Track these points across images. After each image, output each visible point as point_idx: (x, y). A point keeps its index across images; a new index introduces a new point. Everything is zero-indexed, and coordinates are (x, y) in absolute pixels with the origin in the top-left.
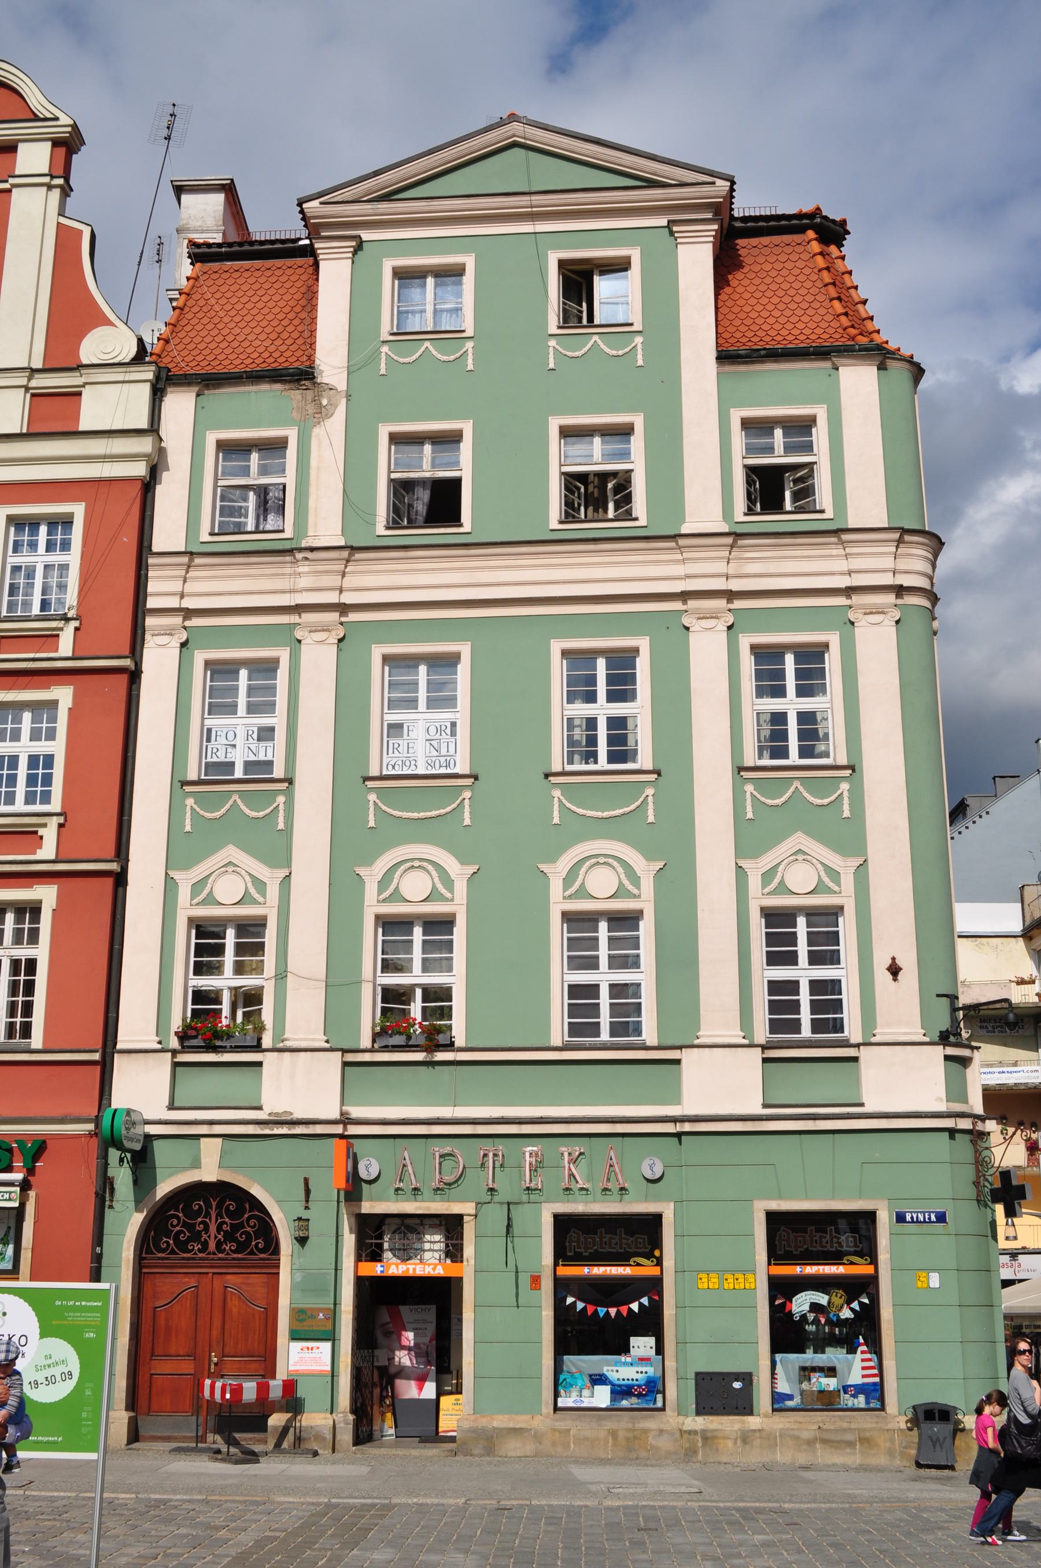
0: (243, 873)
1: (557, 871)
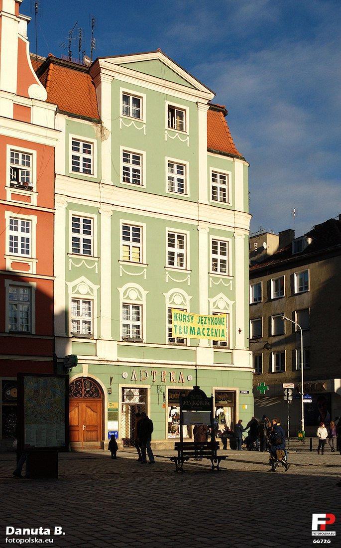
1: (167, 295)
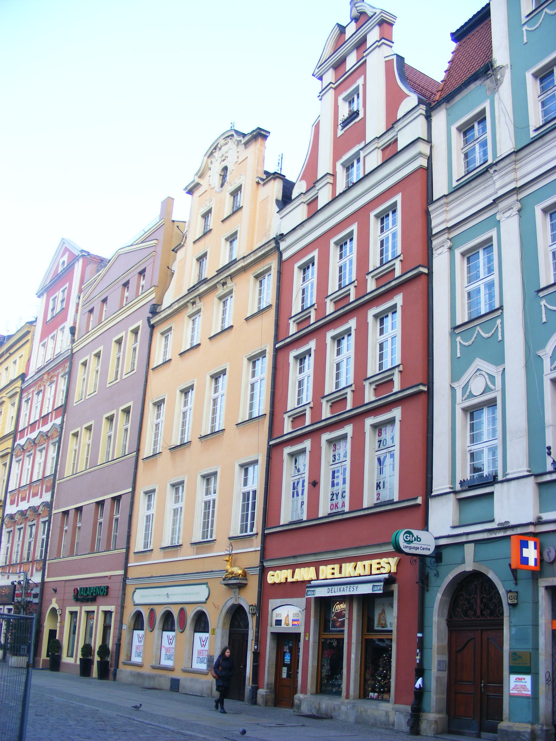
0: (484, 373)
